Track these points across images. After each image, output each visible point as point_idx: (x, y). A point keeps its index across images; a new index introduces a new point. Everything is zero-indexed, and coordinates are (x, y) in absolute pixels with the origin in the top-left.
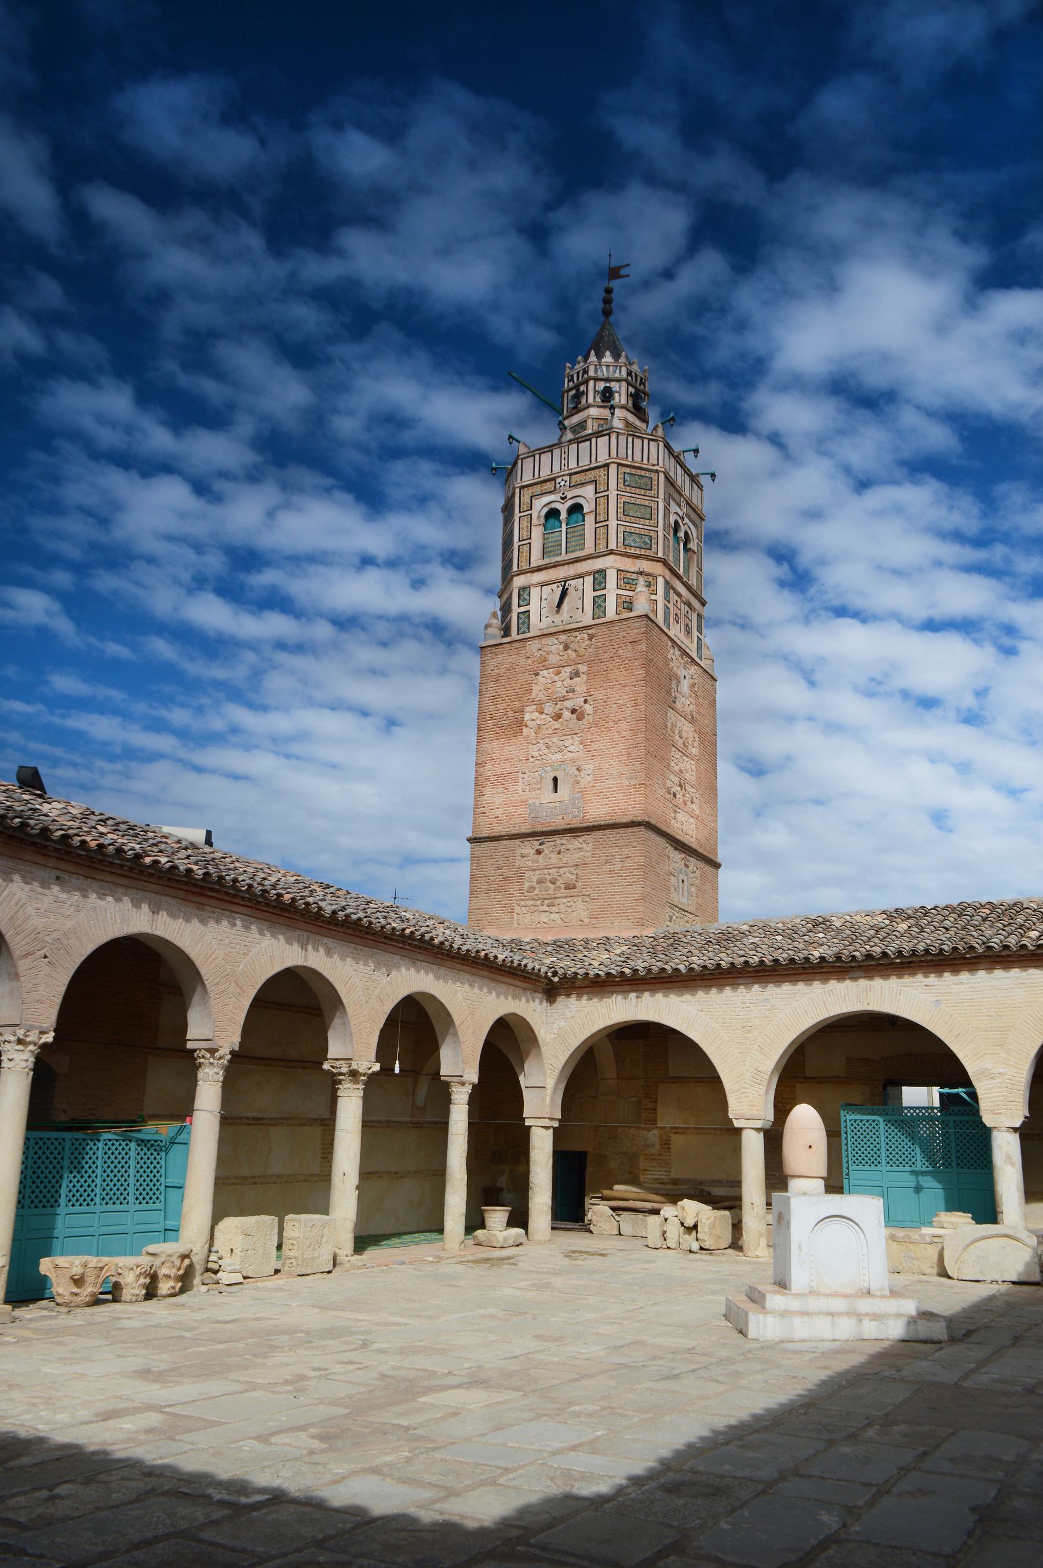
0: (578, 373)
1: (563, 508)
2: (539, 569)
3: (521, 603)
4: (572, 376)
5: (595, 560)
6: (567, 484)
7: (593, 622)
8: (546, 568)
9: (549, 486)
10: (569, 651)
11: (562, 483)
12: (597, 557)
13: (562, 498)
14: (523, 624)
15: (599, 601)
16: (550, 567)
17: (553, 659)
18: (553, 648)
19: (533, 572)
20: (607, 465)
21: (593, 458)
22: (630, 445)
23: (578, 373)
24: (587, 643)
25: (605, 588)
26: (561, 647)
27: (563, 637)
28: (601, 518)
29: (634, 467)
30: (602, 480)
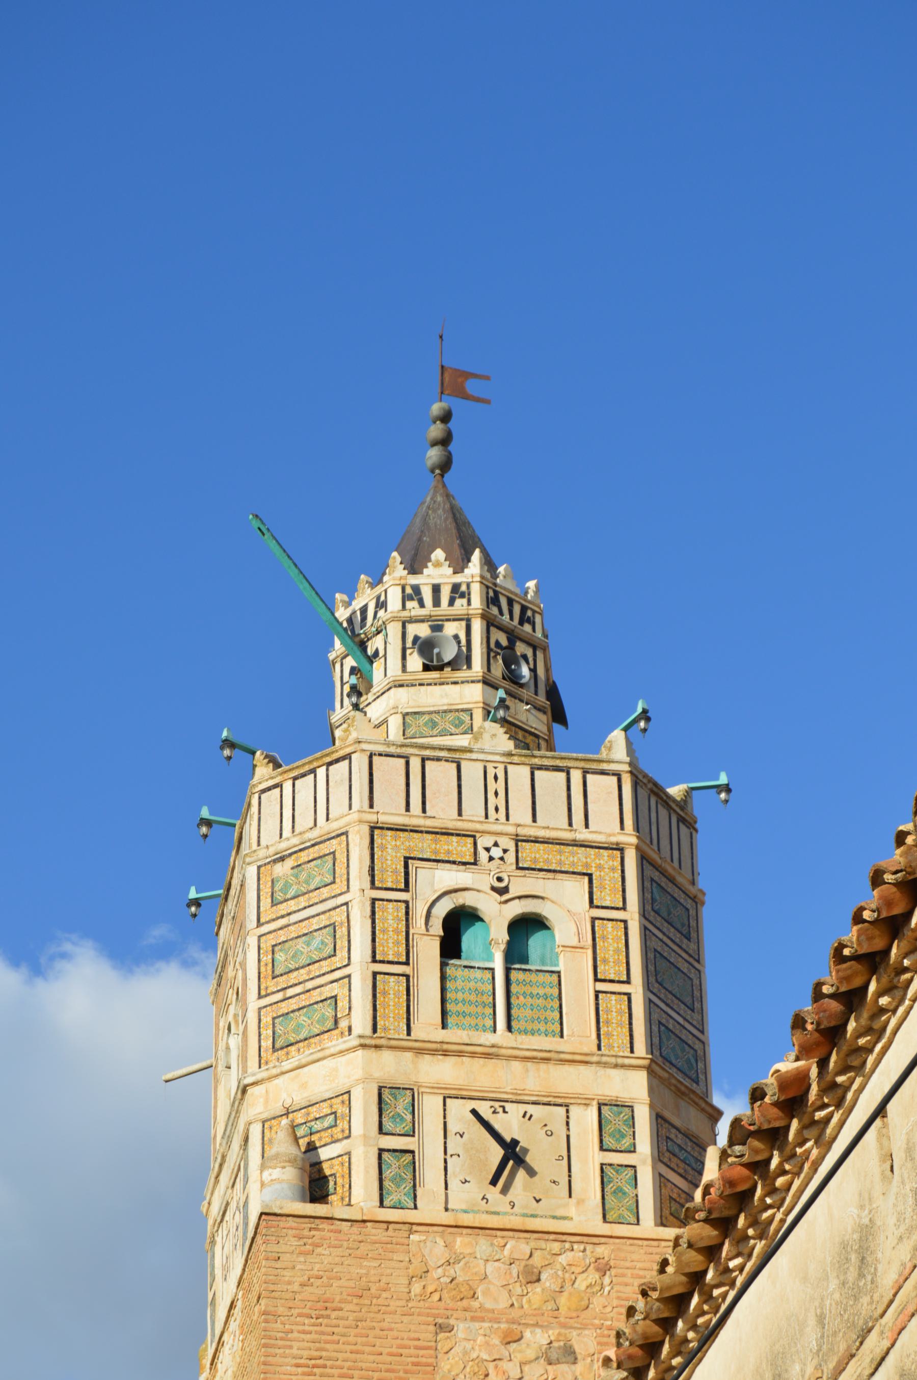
0: (436, 589)
1: (497, 916)
2: (443, 1051)
3: (388, 1125)
4: (417, 589)
5: (601, 1071)
6: (510, 857)
7: (606, 1229)
8: (460, 1054)
9: (461, 849)
10: (538, 1288)
11: (496, 853)
12: (606, 1065)
13: (493, 889)
14: (398, 1180)
15: (621, 1180)
16: (473, 1055)
17: (493, 1297)
18: (491, 1268)
19: (420, 1052)
20: (620, 849)
21: (578, 817)
22: (653, 815)
23: (436, 589)
24: (593, 1276)
25: (632, 1150)
26: (515, 1270)
27: (518, 1247)
28: (609, 970)
29: (663, 873)
30: (607, 880)
